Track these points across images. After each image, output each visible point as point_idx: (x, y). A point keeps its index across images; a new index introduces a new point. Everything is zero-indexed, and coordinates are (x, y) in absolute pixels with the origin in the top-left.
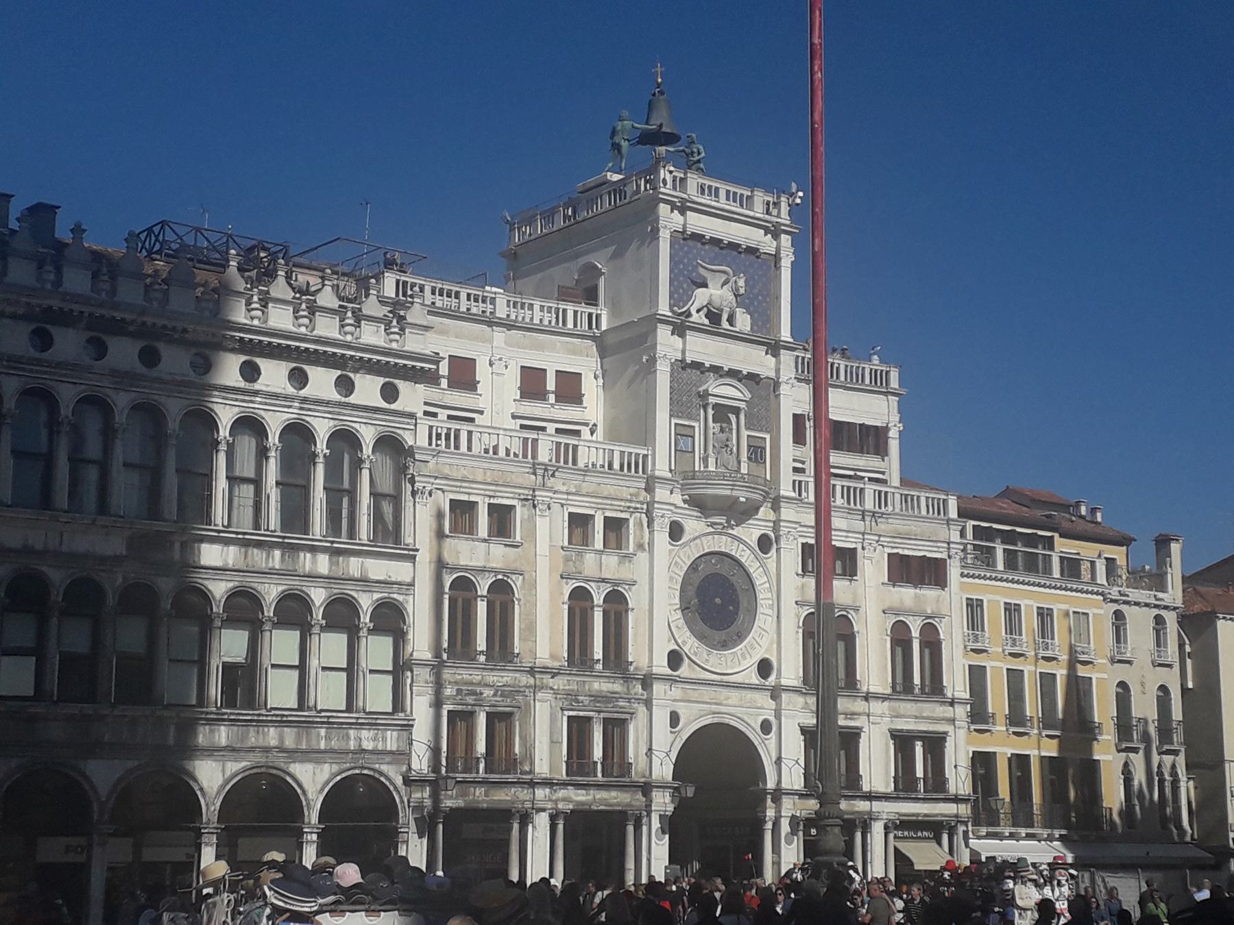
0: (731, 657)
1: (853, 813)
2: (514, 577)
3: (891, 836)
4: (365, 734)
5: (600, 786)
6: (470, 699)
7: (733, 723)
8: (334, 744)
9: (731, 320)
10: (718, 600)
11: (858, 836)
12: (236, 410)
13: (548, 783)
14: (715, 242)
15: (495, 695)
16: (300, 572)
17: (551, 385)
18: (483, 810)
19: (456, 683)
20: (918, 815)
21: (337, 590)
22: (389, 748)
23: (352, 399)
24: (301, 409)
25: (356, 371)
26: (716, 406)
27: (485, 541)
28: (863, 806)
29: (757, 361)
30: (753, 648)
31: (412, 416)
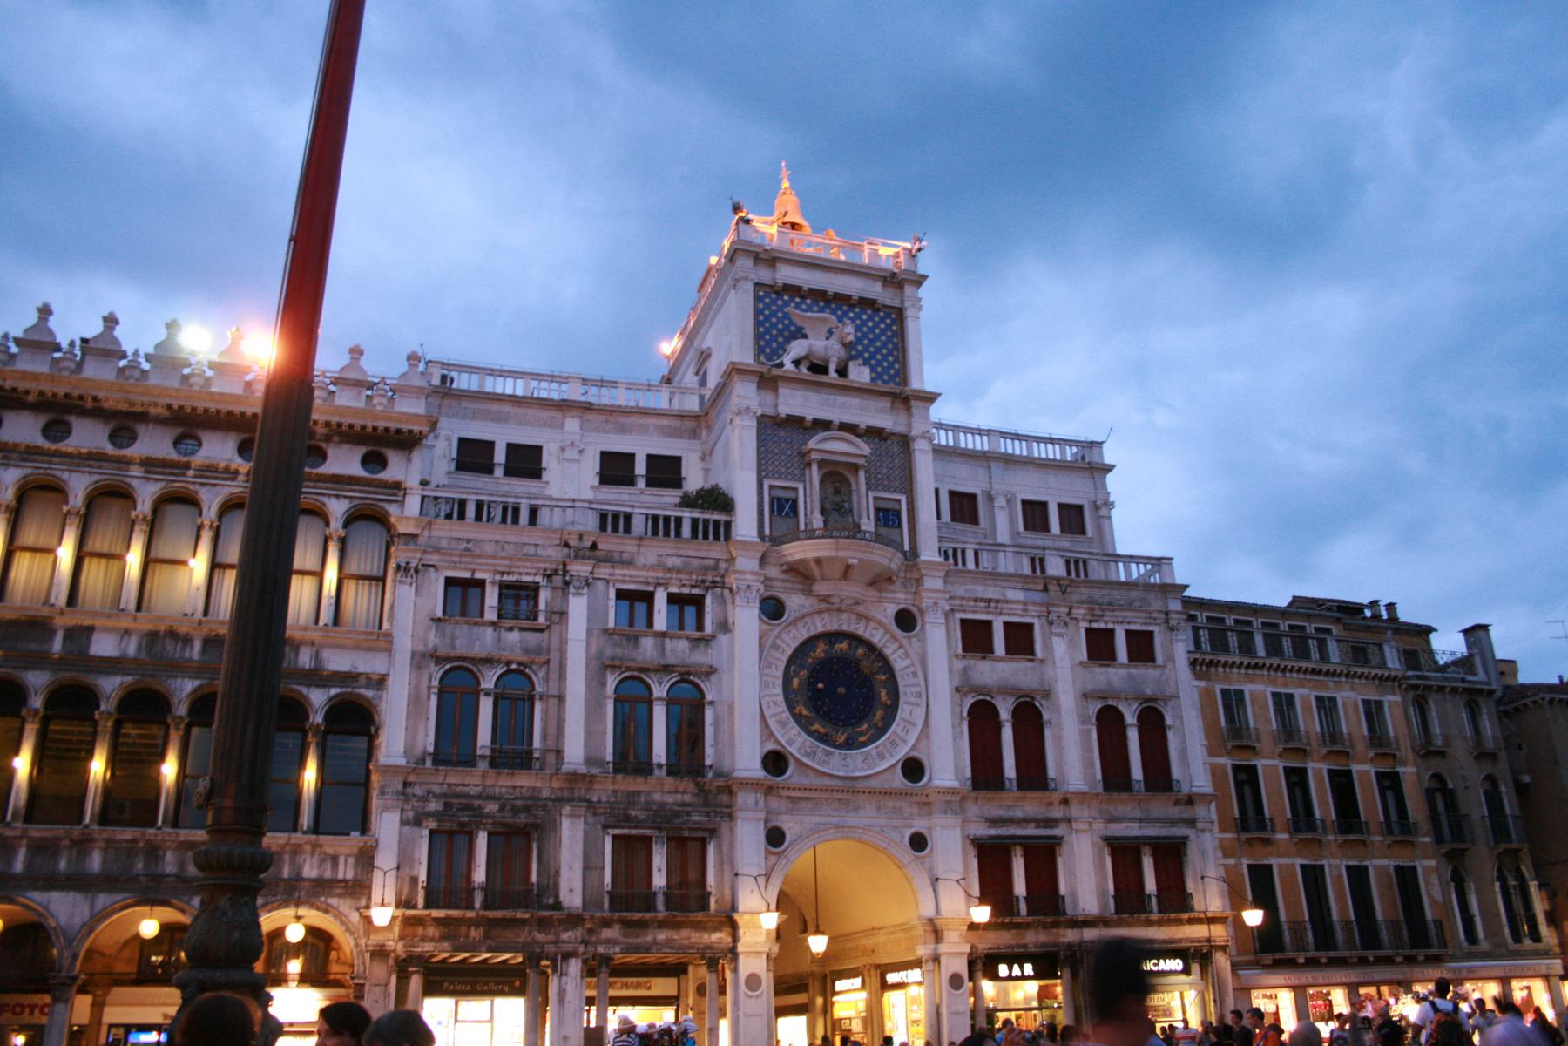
0: (860, 759)
1: (1056, 945)
5: (662, 925)
9: (843, 372)
10: (841, 690)
12: (160, 485)
13: (574, 920)
15: (502, 809)
19: (444, 795)
22: (341, 876)
25: (328, 439)
26: (821, 463)
30: (893, 743)
31: (397, 486)
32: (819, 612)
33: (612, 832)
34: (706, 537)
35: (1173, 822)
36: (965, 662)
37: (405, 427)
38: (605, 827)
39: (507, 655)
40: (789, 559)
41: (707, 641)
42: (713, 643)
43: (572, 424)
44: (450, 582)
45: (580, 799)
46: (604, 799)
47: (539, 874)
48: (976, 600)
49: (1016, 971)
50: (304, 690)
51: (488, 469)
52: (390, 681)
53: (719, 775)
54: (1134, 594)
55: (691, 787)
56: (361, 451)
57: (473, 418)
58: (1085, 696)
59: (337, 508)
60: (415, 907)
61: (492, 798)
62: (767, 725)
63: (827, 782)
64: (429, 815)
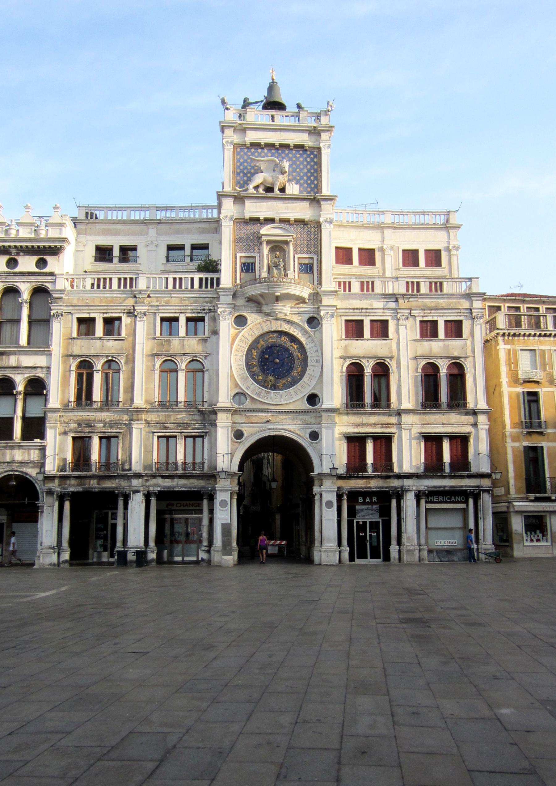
1: (387, 487)
3: (423, 502)
5: (181, 477)
6: (87, 430)
7: (285, 434)
9: (282, 190)
10: (278, 361)
11: (394, 503)
13: (138, 476)
14: (270, 146)
15: (104, 426)
18: (95, 493)
19: (78, 420)
20: (445, 487)
23: (17, 270)
25: (18, 254)
26: (268, 242)
28: (396, 483)
29: (302, 211)
31: (52, 274)
35: (463, 424)
36: (346, 343)
37: (53, 245)
38: (153, 433)
40: (248, 295)
42: (209, 340)
45: (141, 420)
46: (153, 420)
47: (122, 455)
48: (354, 309)
49: (368, 500)
50: (12, 376)
54: (451, 300)
58: (416, 358)
60: (65, 471)
61: (100, 421)
63: (266, 407)
64: (71, 429)
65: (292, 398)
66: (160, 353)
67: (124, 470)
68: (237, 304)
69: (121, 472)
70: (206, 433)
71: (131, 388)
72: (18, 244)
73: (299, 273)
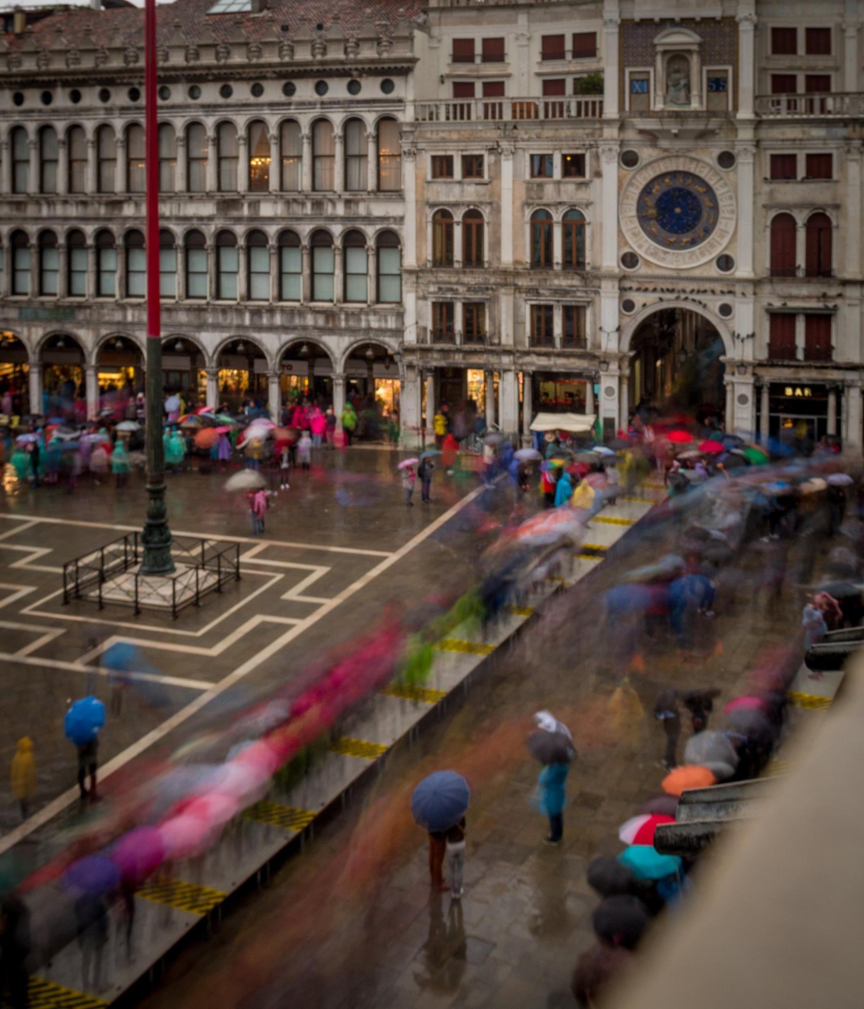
2: (483, 207)
4: (372, 318)
5: (559, 355)
8: (352, 323)
10: (678, 210)
12: (279, 116)
15: (469, 290)
16: (325, 215)
17: (569, 45)
19: (438, 283)
21: (349, 225)
23: (361, 96)
24: (322, 108)
25: (360, 76)
26: (665, 53)
27: (459, 183)
31: (400, 101)
32: (663, 158)
33: (529, 302)
34: (586, 114)
37: (399, 65)
38: (526, 300)
39: (467, 199)
41: (586, 184)
42: (591, 185)
43: (523, 18)
44: (434, 158)
50: (363, 227)
51: (470, 59)
52: (406, 220)
53: (594, 268)
55: (577, 277)
56: (380, 79)
57: (461, 23)
59: (370, 118)
61: (463, 284)
62: (624, 237)
64: (430, 293)
65: (698, 260)
66: (530, 201)
67: (492, 344)
68: (626, 138)
69: (490, 348)
70: (589, 302)
71: (496, 244)
72: (360, 67)
73: (708, 91)
